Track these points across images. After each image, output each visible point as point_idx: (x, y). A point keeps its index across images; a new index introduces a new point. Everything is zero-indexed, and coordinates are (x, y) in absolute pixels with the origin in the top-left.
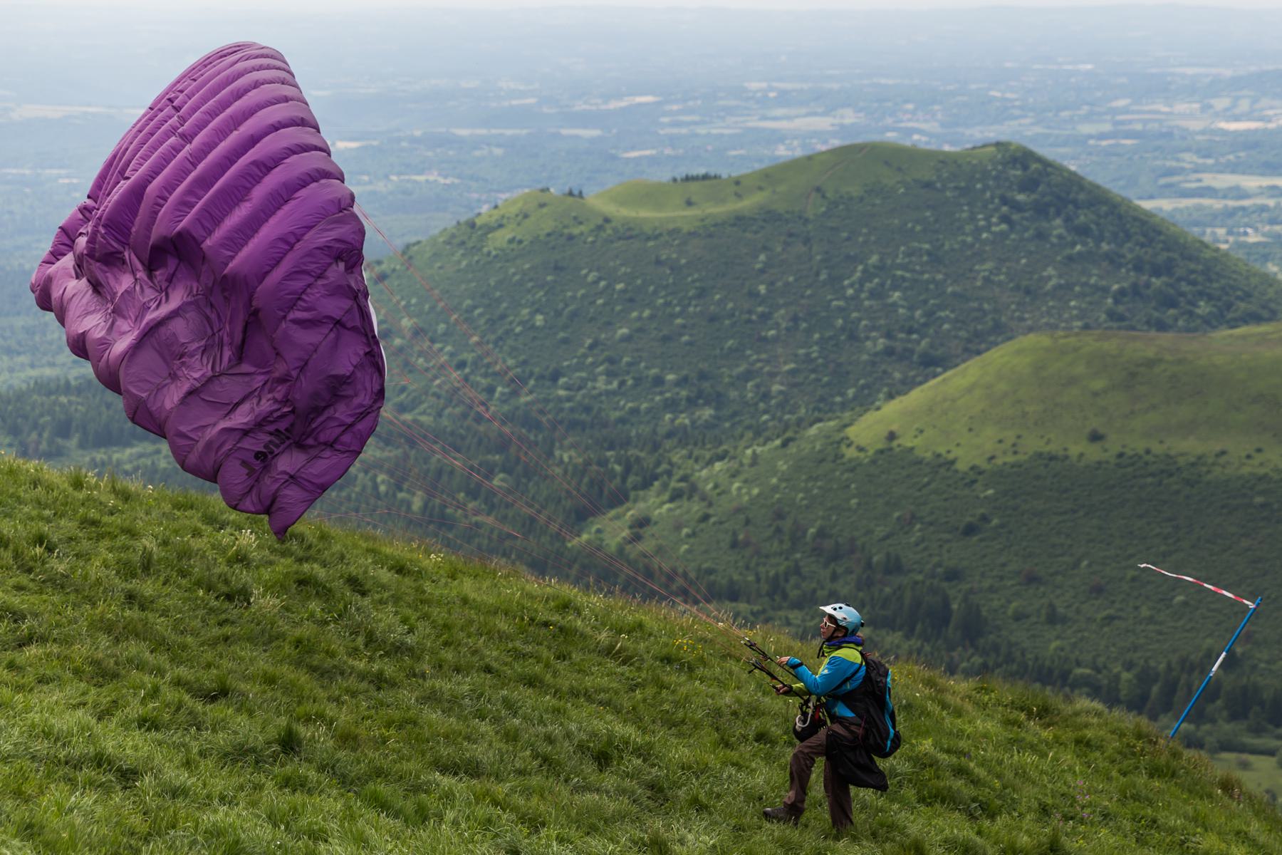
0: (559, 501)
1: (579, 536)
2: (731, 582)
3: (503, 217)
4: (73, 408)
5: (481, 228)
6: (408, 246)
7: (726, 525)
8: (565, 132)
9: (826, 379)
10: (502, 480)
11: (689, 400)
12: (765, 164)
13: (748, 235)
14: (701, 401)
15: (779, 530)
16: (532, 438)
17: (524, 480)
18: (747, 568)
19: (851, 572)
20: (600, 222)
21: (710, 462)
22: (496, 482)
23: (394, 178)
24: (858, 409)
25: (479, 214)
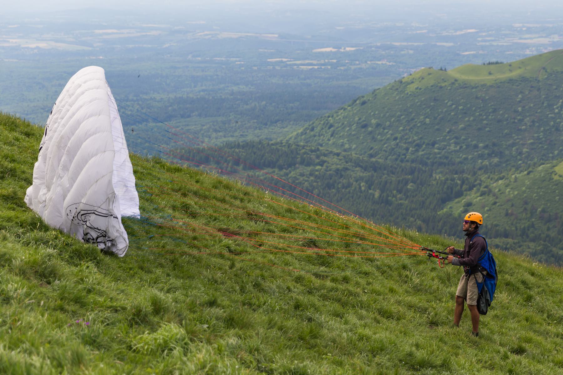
0: (435, 195)
1: (442, 209)
2: (505, 230)
3: (414, 79)
4: (241, 154)
5: (404, 83)
6: (375, 90)
7: (504, 207)
8: (438, 44)
9: (546, 147)
10: (412, 186)
11: (489, 154)
12: (521, 58)
13: (514, 87)
14: (493, 155)
15: (525, 209)
16: (424, 169)
17: (420, 186)
18: (512, 224)
19: (556, 227)
20: (453, 81)
21: (497, 180)
22: (409, 187)
23: (369, 62)
24: (559, 159)
25: (404, 77)
